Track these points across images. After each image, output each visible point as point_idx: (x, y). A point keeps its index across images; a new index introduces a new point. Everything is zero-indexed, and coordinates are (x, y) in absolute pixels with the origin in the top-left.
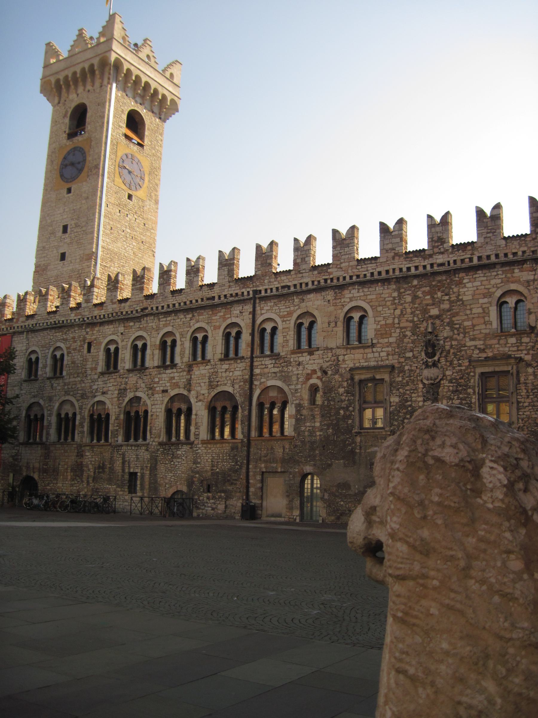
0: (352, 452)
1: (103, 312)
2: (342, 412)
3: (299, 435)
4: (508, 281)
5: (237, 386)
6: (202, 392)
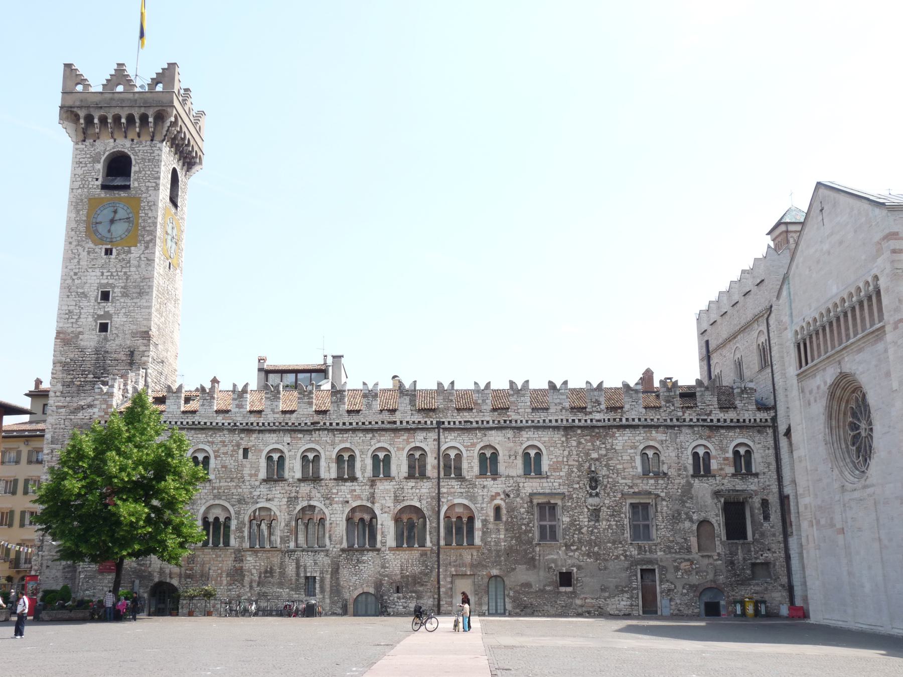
0: (533, 559)
1: (261, 421)
2: (523, 527)
3: (485, 544)
5: (424, 502)
6: (387, 505)
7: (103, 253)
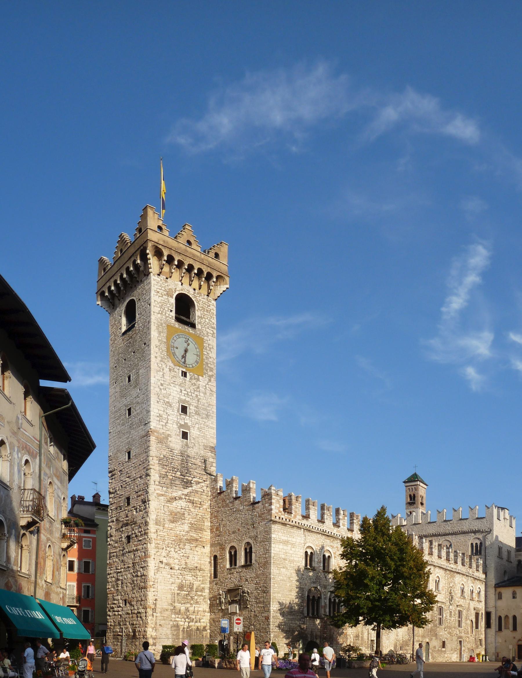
4: (462, 580)
7: (180, 375)
